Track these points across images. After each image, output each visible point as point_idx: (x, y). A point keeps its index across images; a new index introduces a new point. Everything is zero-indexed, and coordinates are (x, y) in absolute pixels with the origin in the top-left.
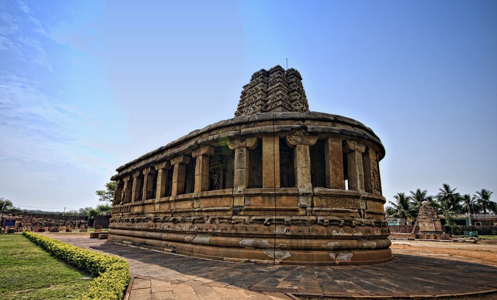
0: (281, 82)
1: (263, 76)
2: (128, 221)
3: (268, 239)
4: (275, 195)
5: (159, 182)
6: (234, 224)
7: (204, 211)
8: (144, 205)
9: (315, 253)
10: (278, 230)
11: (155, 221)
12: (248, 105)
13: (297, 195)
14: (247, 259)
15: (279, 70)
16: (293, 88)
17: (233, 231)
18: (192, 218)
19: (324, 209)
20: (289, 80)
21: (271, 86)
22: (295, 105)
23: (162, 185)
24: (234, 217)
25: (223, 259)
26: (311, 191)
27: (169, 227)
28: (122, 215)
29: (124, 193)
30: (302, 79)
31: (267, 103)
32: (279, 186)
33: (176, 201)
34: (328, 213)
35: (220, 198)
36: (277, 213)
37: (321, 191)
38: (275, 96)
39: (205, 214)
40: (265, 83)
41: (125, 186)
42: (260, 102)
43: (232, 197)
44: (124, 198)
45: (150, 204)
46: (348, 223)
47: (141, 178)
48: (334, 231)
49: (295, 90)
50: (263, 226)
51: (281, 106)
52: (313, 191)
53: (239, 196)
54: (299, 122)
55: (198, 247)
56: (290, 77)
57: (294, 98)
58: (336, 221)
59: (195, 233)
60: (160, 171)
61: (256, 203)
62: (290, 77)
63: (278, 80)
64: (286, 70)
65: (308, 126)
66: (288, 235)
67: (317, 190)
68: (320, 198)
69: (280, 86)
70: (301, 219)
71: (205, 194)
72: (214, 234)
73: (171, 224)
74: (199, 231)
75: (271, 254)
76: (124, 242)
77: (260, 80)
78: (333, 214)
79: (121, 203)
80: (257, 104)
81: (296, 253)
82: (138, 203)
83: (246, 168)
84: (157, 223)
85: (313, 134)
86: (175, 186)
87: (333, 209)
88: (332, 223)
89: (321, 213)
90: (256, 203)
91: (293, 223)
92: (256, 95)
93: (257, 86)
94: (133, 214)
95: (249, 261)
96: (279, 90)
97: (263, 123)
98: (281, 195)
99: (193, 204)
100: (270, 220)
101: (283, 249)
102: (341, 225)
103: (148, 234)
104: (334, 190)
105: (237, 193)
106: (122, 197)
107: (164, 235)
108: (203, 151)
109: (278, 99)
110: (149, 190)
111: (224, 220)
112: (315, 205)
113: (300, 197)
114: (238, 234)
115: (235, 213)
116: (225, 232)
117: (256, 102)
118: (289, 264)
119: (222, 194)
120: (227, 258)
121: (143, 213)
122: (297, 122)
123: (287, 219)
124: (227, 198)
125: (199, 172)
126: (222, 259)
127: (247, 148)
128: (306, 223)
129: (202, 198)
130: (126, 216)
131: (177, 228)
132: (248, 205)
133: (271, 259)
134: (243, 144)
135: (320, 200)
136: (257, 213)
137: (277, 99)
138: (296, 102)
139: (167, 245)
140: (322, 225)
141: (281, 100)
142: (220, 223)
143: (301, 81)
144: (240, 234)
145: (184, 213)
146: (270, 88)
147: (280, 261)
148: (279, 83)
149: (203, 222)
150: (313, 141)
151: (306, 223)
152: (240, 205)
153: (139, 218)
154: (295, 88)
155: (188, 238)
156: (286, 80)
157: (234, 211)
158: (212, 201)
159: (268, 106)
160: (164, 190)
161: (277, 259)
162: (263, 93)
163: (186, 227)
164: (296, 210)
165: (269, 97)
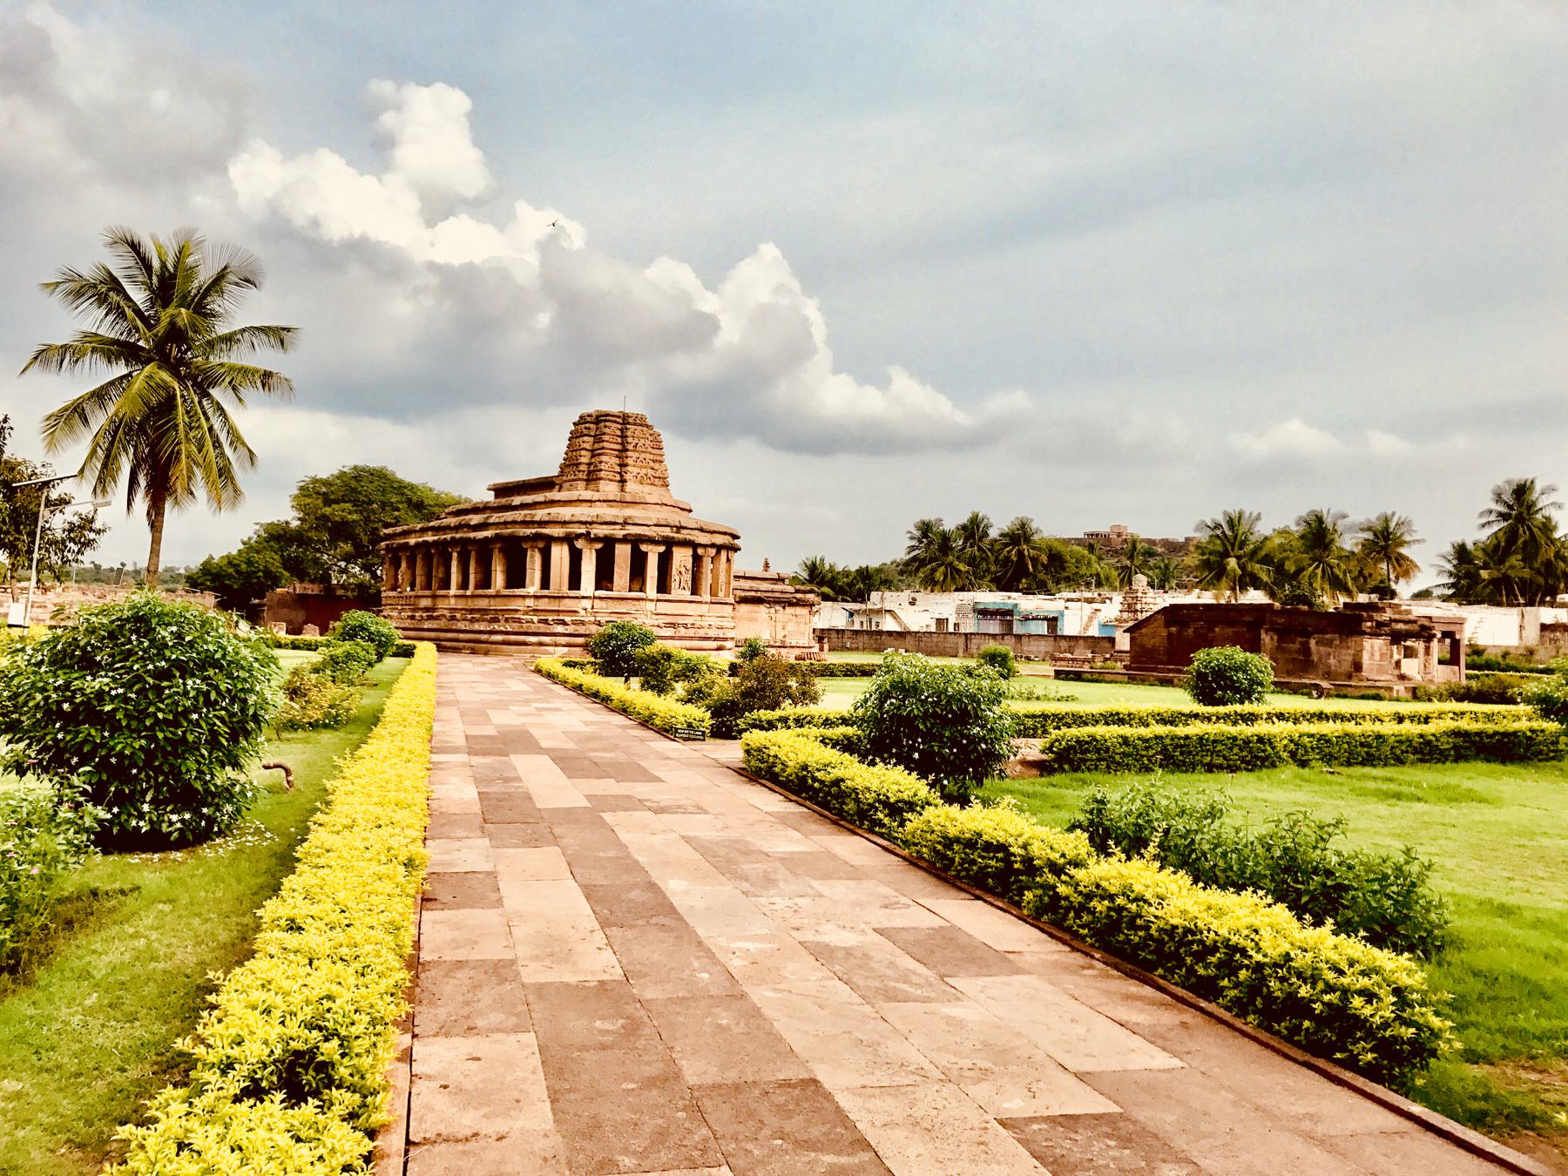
2: (413, 617)
10: (560, 629)
11: (453, 618)
33: (473, 596)
41: (404, 565)
43: (524, 597)
61: (543, 604)
82: (427, 593)
85: (597, 539)
91: (574, 623)
103: (442, 635)
115: (526, 613)
121: (433, 609)
123: (568, 619)
131: (476, 627)
150: (599, 546)
155: (484, 637)
163: (482, 626)
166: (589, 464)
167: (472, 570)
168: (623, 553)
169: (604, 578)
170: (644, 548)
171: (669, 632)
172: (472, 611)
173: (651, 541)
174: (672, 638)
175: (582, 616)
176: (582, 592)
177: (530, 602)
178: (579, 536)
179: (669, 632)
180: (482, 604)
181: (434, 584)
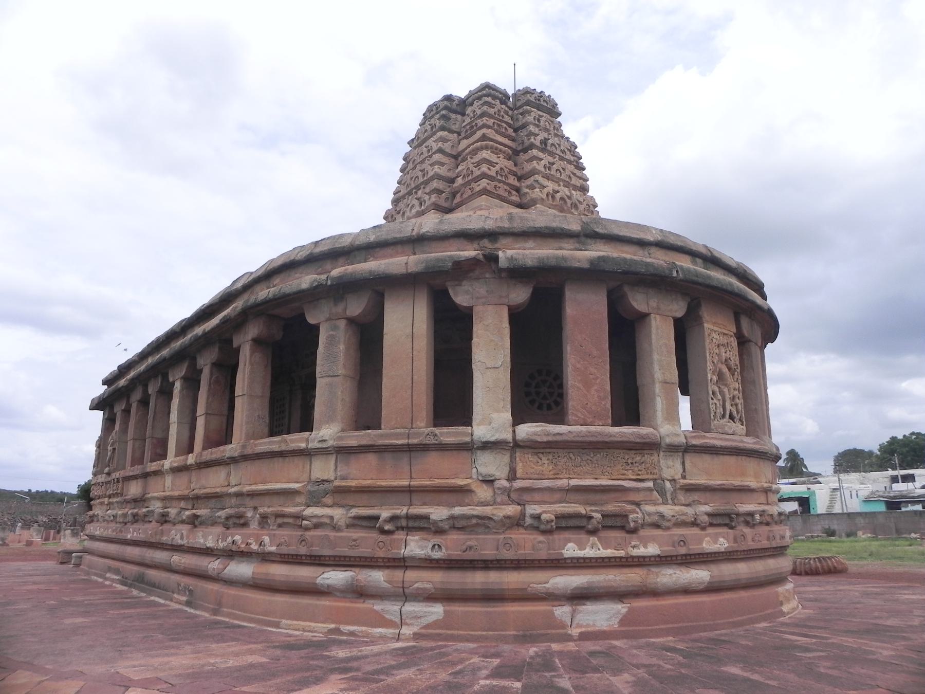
0: (488, 127)
1: (447, 113)
3: (387, 572)
4: (409, 449)
5: (174, 416)
6: (307, 529)
7: (248, 495)
8: (146, 475)
9: (513, 608)
11: (164, 519)
12: (410, 193)
13: (469, 448)
14: (333, 626)
15: (487, 95)
16: (526, 141)
17: (303, 550)
18: (222, 514)
19: (546, 483)
20: (517, 119)
21: (466, 138)
22: (532, 187)
23: (179, 423)
24: (309, 511)
25: (279, 622)
26: (509, 437)
27: (182, 538)
28: (109, 504)
29: (112, 445)
30: (560, 114)
31: (455, 185)
32: (423, 424)
34: (557, 496)
35: (281, 459)
36: (415, 497)
37: (535, 434)
38: (471, 166)
39: (249, 502)
40: (451, 131)
41: (117, 427)
42: (435, 184)
43: (306, 454)
44: (112, 458)
45: (156, 473)
46: (617, 523)
47: (144, 402)
48: (570, 545)
49: (532, 146)
50: (374, 535)
51: (485, 192)
52: (514, 432)
53: (323, 452)
54: (481, 243)
55: (232, 591)
56: (521, 110)
57: (528, 167)
58: (578, 516)
59: (231, 554)
60: (178, 385)
62: (521, 110)
63: (480, 122)
64: (511, 92)
65: (501, 254)
66: (437, 561)
67: (526, 430)
68: (537, 454)
69: (484, 138)
70: (475, 513)
71: (249, 451)
72: (265, 557)
73: (185, 529)
74: (234, 548)
75: (391, 609)
76: (108, 575)
77: (438, 124)
78: (572, 496)
79: (106, 470)
80: (427, 190)
81: (459, 608)
83: (345, 376)
84: (166, 527)
86: (200, 422)
87: (573, 482)
88: (569, 524)
89: (537, 496)
90: (362, 472)
92: (426, 166)
93: (430, 142)
94: (127, 502)
95: (337, 631)
96: (482, 148)
97: (389, 251)
98: (424, 448)
99: (229, 474)
100: (394, 518)
101: (430, 598)
102: (590, 526)
104: (583, 428)
105: (314, 445)
106: (109, 453)
107: (177, 559)
108: (253, 331)
109: (477, 173)
110: (159, 435)
111: (286, 520)
112: (519, 473)
113: (479, 452)
114: (315, 556)
115: (315, 500)
116: (284, 550)
117: (426, 183)
118: (439, 637)
119: (284, 447)
120: (289, 622)
121: (139, 501)
122: (476, 242)
123: (438, 513)
124: (296, 460)
125: (243, 390)
126: (277, 625)
127: (351, 321)
128: (491, 524)
129: (245, 457)
130: (116, 505)
132: (344, 478)
133: (389, 624)
134: (339, 309)
135: (534, 459)
136: (364, 499)
137: (475, 175)
138: (532, 179)
139: (179, 585)
140: (537, 528)
141: (484, 176)
142: (280, 526)
143: (559, 119)
144: (320, 556)
145: (213, 500)
146: (465, 143)
147: (415, 629)
148: (484, 131)
149: (245, 525)
150: (520, 295)
151: (491, 524)
152: (325, 478)
153: (136, 511)
154: (532, 140)
155: (213, 565)
156: (507, 119)
157: (310, 492)
158: (263, 467)
159: (458, 192)
160: (186, 434)
161: (407, 624)
162: (445, 160)
163: (208, 538)
164: (462, 492)
165: (460, 168)
166: (452, 181)
167: (201, 409)
168: (584, 317)
169: (538, 390)
170: (639, 301)
171: (718, 542)
172: (197, 499)
173: (659, 282)
174: (728, 556)
175: (483, 503)
176: (480, 431)
177: (323, 469)
178: (462, 270)
179: (718, 542)
180: (214, 481)
181: (148, 455)
